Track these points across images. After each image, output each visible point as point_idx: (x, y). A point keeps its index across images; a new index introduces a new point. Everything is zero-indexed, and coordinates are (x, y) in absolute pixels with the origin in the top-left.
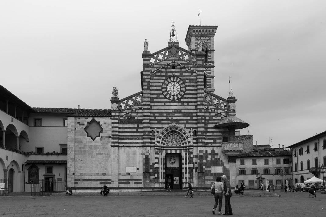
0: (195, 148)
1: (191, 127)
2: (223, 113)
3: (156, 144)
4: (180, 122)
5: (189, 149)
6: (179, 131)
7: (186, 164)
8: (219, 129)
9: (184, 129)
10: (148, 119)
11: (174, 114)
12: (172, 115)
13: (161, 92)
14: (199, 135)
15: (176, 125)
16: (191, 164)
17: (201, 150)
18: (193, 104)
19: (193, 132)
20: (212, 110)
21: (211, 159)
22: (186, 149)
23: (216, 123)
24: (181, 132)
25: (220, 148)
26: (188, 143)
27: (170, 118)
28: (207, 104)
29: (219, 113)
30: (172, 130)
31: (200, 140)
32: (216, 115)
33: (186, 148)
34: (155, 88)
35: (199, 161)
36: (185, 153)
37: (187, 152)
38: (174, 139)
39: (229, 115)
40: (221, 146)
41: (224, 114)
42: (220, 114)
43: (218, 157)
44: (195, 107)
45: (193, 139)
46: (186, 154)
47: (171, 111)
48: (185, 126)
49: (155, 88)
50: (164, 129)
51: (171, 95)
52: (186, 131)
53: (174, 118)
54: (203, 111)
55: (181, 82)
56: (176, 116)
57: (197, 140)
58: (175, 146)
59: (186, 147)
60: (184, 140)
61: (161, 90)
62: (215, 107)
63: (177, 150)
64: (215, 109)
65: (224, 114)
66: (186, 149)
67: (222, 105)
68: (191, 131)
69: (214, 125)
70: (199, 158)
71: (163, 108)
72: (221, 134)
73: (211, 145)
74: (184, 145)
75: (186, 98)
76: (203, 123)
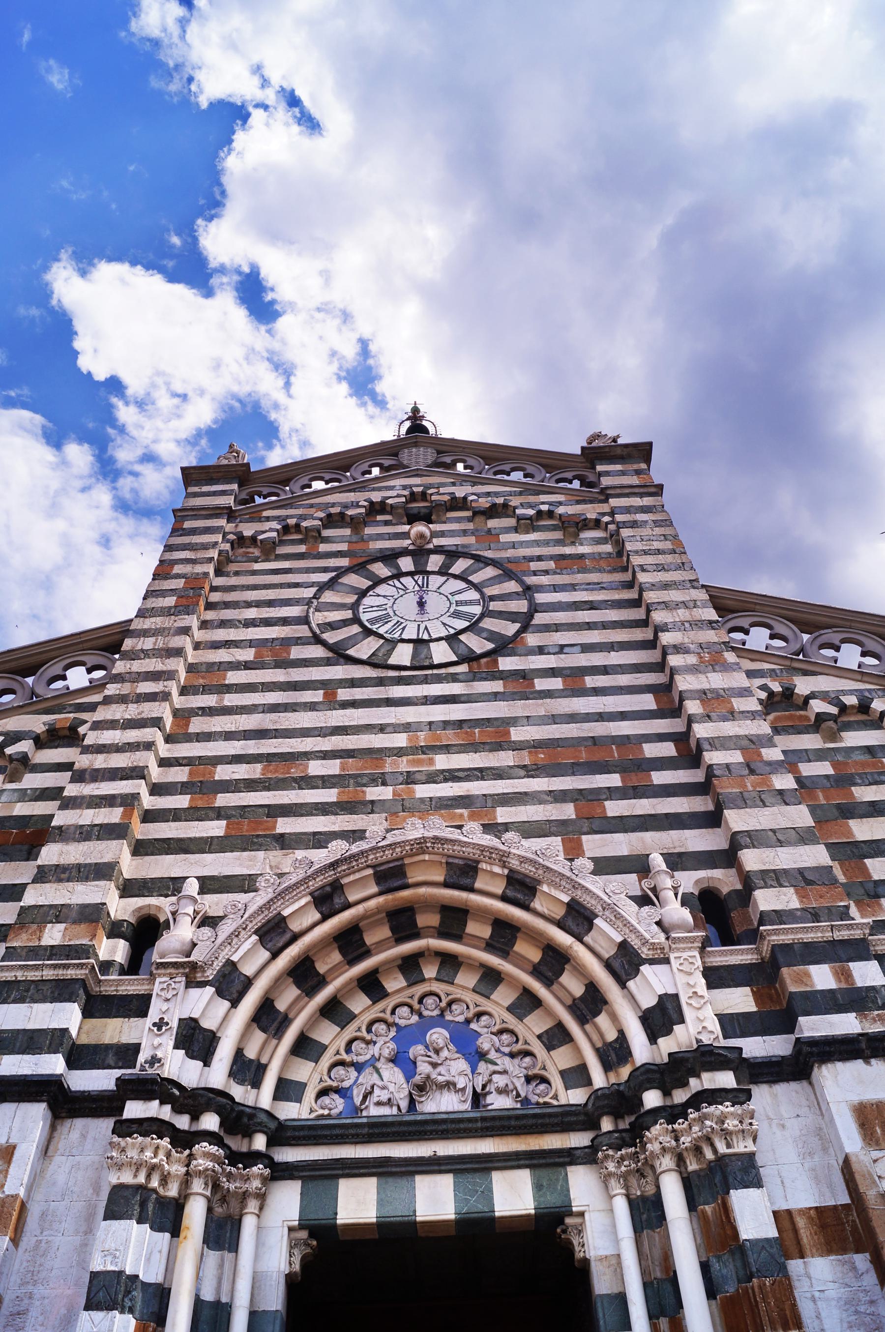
3: (154, 1060)
5: (673, 1114)
10: (109, 801)
11: (431, 762)
13: (302, 631)
26: (653, 1038)
34: (252, 613)
36: (621, 1206)
38: (440, 1020)
49: (252, 613)
51: (392, 644)
55: (489, 572)
58: (467, 1106)
61: (305, 620)
71: (305, 719)
75: (541, 650)
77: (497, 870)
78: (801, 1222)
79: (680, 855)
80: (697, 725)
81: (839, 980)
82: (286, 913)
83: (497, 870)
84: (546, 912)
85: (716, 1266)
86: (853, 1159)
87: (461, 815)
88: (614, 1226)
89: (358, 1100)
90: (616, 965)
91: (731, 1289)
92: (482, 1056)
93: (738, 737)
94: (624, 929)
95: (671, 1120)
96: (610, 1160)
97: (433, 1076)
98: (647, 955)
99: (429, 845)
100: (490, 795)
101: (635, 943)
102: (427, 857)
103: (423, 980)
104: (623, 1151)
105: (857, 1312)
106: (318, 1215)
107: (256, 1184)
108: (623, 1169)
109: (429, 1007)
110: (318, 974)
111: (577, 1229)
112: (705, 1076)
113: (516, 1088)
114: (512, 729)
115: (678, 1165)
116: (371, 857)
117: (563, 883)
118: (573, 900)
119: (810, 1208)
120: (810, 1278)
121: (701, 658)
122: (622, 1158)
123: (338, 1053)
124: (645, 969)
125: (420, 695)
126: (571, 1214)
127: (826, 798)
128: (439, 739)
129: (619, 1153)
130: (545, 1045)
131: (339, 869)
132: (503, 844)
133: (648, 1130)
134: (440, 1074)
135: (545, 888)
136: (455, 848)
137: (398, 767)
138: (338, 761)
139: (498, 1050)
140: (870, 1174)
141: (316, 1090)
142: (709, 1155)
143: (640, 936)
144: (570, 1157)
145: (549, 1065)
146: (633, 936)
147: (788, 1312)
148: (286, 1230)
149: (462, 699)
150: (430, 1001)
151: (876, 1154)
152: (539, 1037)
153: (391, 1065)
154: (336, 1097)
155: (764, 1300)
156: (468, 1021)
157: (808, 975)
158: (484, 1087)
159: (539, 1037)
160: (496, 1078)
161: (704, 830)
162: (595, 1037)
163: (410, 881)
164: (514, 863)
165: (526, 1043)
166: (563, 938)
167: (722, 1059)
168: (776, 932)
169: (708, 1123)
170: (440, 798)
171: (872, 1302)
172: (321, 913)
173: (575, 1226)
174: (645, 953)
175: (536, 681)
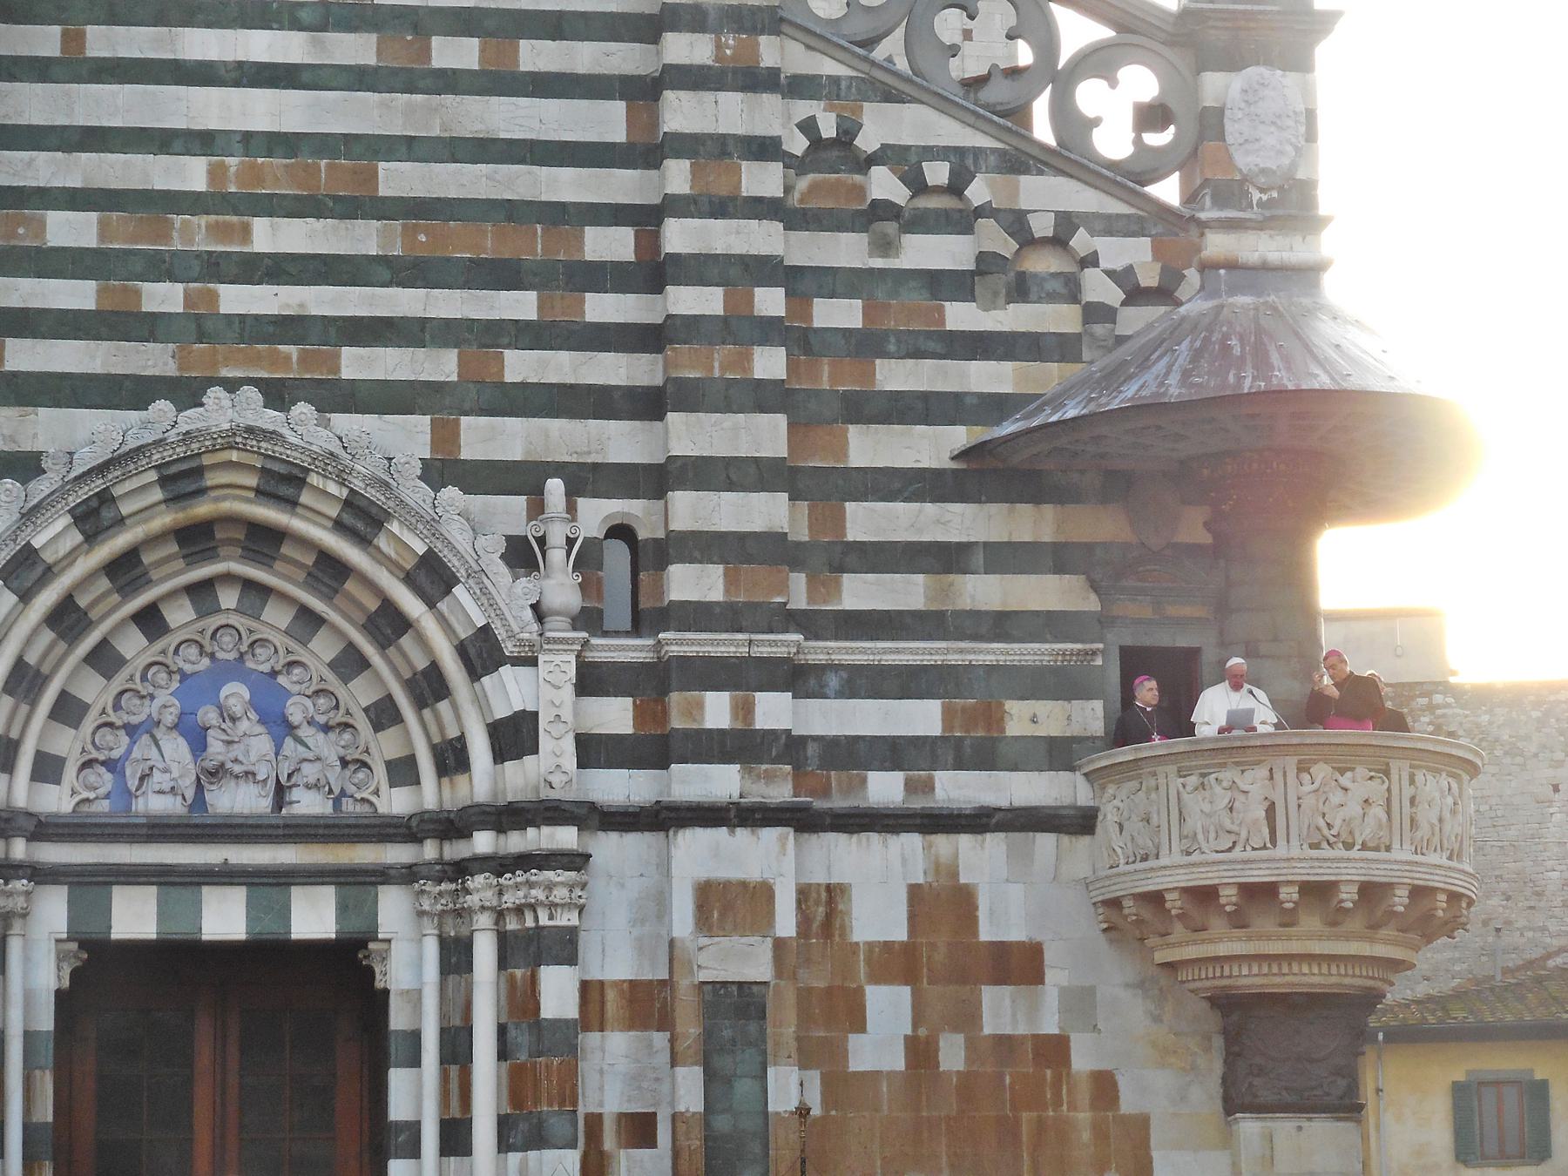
0: (609, 848)
1: (558, 469)
2: (1110, 226)
4: (356, 364)
6: (339, 526)
7: (455, 1138)
8: (1048, 510)
9: (416, 493)
12: (202, 244)
14: (697, 616)
15: (270, 419)
16: (538, 1140)
17: (727, 885)
18: (585, 57)
19: (587, 559)
20: (918, 185)
21: (920, 1052)
22: (460, 870)
23: (996, 406)
24: (364, 541)
25: (1079, 853)
27: (164, 297)
28: (829, 67)
29: (1042, 226)
30: (203, 509)
31: (717, 710)
32: (987, 263)
33: (456, 850)
35: (689, 1089)
36: (431, 948)
37: (462, 913)
38: (236, 670)
39: (1207, 267)
40: (1082, 822)
41: (1135, 253)
42: (1059, 241)
43: (1034, 1010)
44: (617, 109)
45: (591, 681)
46: (456, 957)
47: (192, 174)
48: (445, 435)
50: (42, 487)
52: (458, 533)
53: (237, 299)
54: (763, 180)
56: (279, 269)
57: (664, 691)
59: (465, 834)
60: (420, 703)
62: (974, 119)
63: (285, 878)
64: (977, 152)
65: (1135, 253)
66: (460, 870)
67: (1090, 96)
68: (557, 534)
69: (959, 436)
70: (690, 1028)
72: (1092, 604)
73: (911, 787)
74: (430, 794)
76: (764, 397)
77: (333, 488)
78: (611, 995)
79: (596, 467)
80: (672, 220)
81: (735, 716)
82: (37, 543)
83: (333, 488)
84: (393, 555)
85: (512, 1033)
86: (678, 944)
87: (288, 358)
88: (420, 958)
89: (132, 784)
90: (472, 652)
91: (523, 1057)
92: (291, 729)
93: (728, 258)
94: (490, 609)
95: (500, 875)
96: (425, 896)
97: (229, 765)
98: (511, 652)
99: (239, 439)
100: (335, 319)
101: (501, 633)
102: (234, 456)
103: (218, 610)
104: (444, 886)
105: (639, 1088)
106: (92, 929)
107: (20, 902)
108: (439, 907)
109: (225, 647)
110: (78, 608)
111: (381, 955)
112: (545, 830)
113: (329, 784)
114: (382, 165)
115: (496, 923)
116: (155, 457)
117: (420, 526)
118: (430, 550)
119: (624, 981)
120: (603, 1051)
121: (719, 47)
122: (440, 894)
123: (104, 712)
124: (506, 671)
125: (229, 58)
126: (376, 939)
127: (832, 378)
128: (258, 176)
129: (438, 888)
130: (371, 721)
131: (110, 476)
132: (345, 448)
133: (472, 876)
134: (236, 761)
135: (394, 527)
136: (276, 448)
137: (191, 241)
138: (93, 216)
139: (311, 722)
140: (690, 962)
141: (79, 763)
142: (530, 923)
143: (507, 626)
144: (383, 875)
145: (373, 750)
146: (499, 625)
147: (568, 1092)
148: (53, 942)
149: (306, 77)
150: (227, 639)
151: (704, 941)
152: (366, 710)
153: (175, 734)
154: (102, 770)
155: (548, 1078)
156: (274, 674)
157: (700, 705)
158: (290, 776)
159: (366, 710)
160: (306, 768)
161: (637, 423)
162: (433, 729)
163: (209, 483)
164: (358, 485)
165: (348, 713)
166: (411, 605)
167: (568, 815)
168: (680, 642)
169: (533, 892)
170: (257, 317)
171: (657, 1079)
172: (83, 532)
173: (377, 951)
174: (509, 648)
175: (436, 41)
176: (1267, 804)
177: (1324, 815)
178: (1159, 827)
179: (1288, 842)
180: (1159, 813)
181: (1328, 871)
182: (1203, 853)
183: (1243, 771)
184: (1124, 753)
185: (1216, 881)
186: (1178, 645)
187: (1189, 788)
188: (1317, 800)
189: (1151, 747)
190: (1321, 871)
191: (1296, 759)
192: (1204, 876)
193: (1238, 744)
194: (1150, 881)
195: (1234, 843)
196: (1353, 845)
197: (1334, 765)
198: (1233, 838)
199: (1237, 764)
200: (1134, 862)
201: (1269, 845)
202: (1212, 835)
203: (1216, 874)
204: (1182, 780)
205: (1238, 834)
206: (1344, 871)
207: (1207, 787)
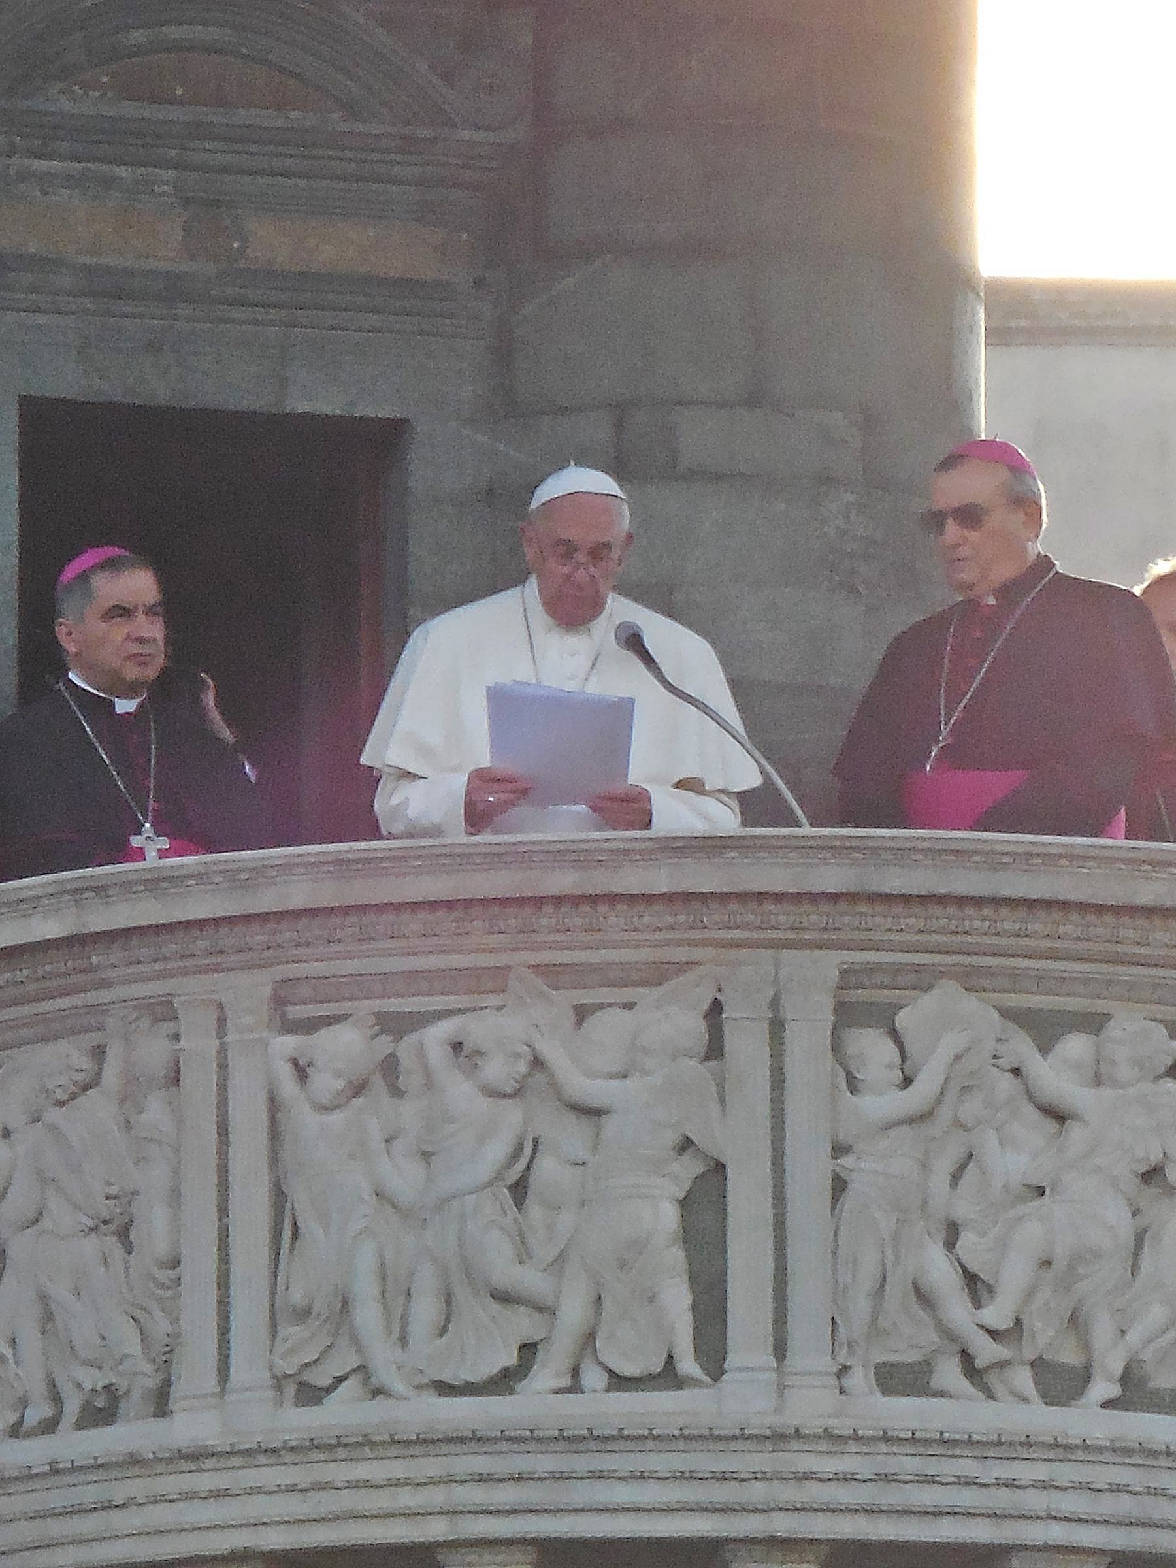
176: (689, 1169)
177: (952, 1233)
178: (175, 1263)
179: (780, 1350)
180: (175, 1196)
181: (966, 1498)
182: (377, 1392)
183: (582, 1013)
184: (34, 903)
185: (436, 1530)
186: (302, 407)
187: (325, 1083)
188: (925, 1166)
189: (155, 884)
190: (928, 1496)
191: (830, 963)
192: (382, 1501)
193: (564, 881)
194: (120, 1521)
195: (528, 1350)
196: (1084, 1376)
197: (1013, 1000)
198: (525, 1325)
199: (551, 973)
200: (49, 1426)
201: (688, 1365)
202: (425, 1310)
203: (437, 1497)
204: (288, 1043)
205: (546, 1310)
206: (1036, 1501)
207: (411, 1081)
